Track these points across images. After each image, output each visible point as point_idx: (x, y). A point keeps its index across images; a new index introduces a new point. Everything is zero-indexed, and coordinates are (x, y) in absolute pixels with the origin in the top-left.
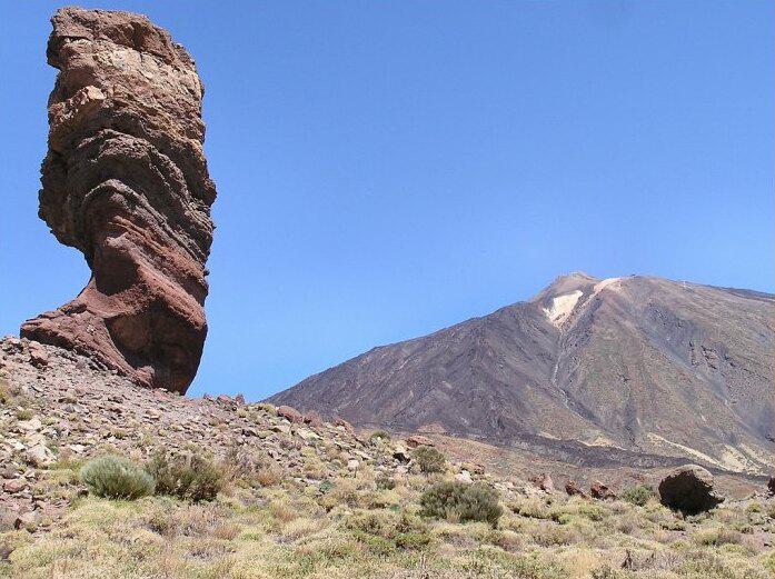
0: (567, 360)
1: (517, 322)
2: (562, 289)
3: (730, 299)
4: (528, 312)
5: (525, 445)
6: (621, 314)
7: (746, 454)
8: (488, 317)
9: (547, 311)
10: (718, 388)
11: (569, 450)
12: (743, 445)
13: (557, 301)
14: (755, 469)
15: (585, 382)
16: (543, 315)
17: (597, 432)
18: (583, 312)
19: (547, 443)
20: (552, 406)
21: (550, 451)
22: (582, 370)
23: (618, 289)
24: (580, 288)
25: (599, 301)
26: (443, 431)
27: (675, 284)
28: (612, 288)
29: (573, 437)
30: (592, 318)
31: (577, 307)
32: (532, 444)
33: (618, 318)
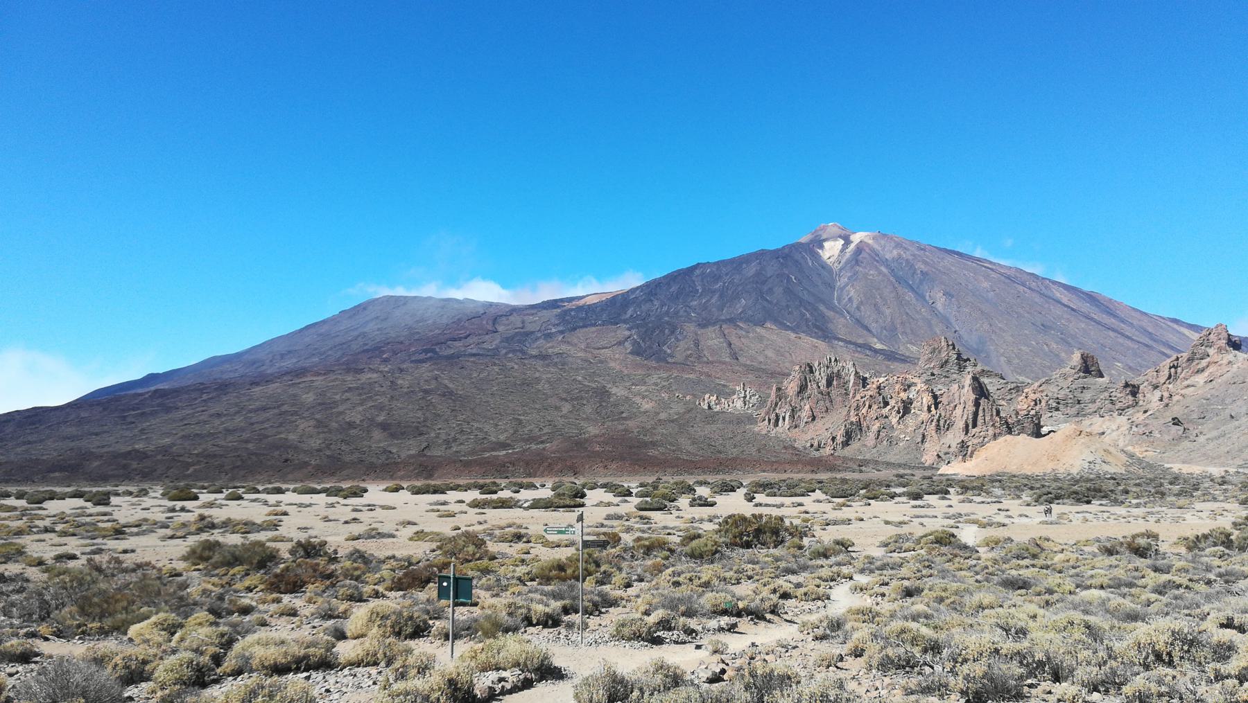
0: (842, 289)
1: (803, 257)
2: (824, 237)
3: (949, 259)
8: (778, 250)
10: (947, 320)
13: (826, 244)
15: (858, 308)
16: (818, 254)
18: (848, 255)
20: (842, 320)
22: (852, 294)
23: (870, 242)
24: (840, 237)
27: (912, 243)
31: (842, 251)
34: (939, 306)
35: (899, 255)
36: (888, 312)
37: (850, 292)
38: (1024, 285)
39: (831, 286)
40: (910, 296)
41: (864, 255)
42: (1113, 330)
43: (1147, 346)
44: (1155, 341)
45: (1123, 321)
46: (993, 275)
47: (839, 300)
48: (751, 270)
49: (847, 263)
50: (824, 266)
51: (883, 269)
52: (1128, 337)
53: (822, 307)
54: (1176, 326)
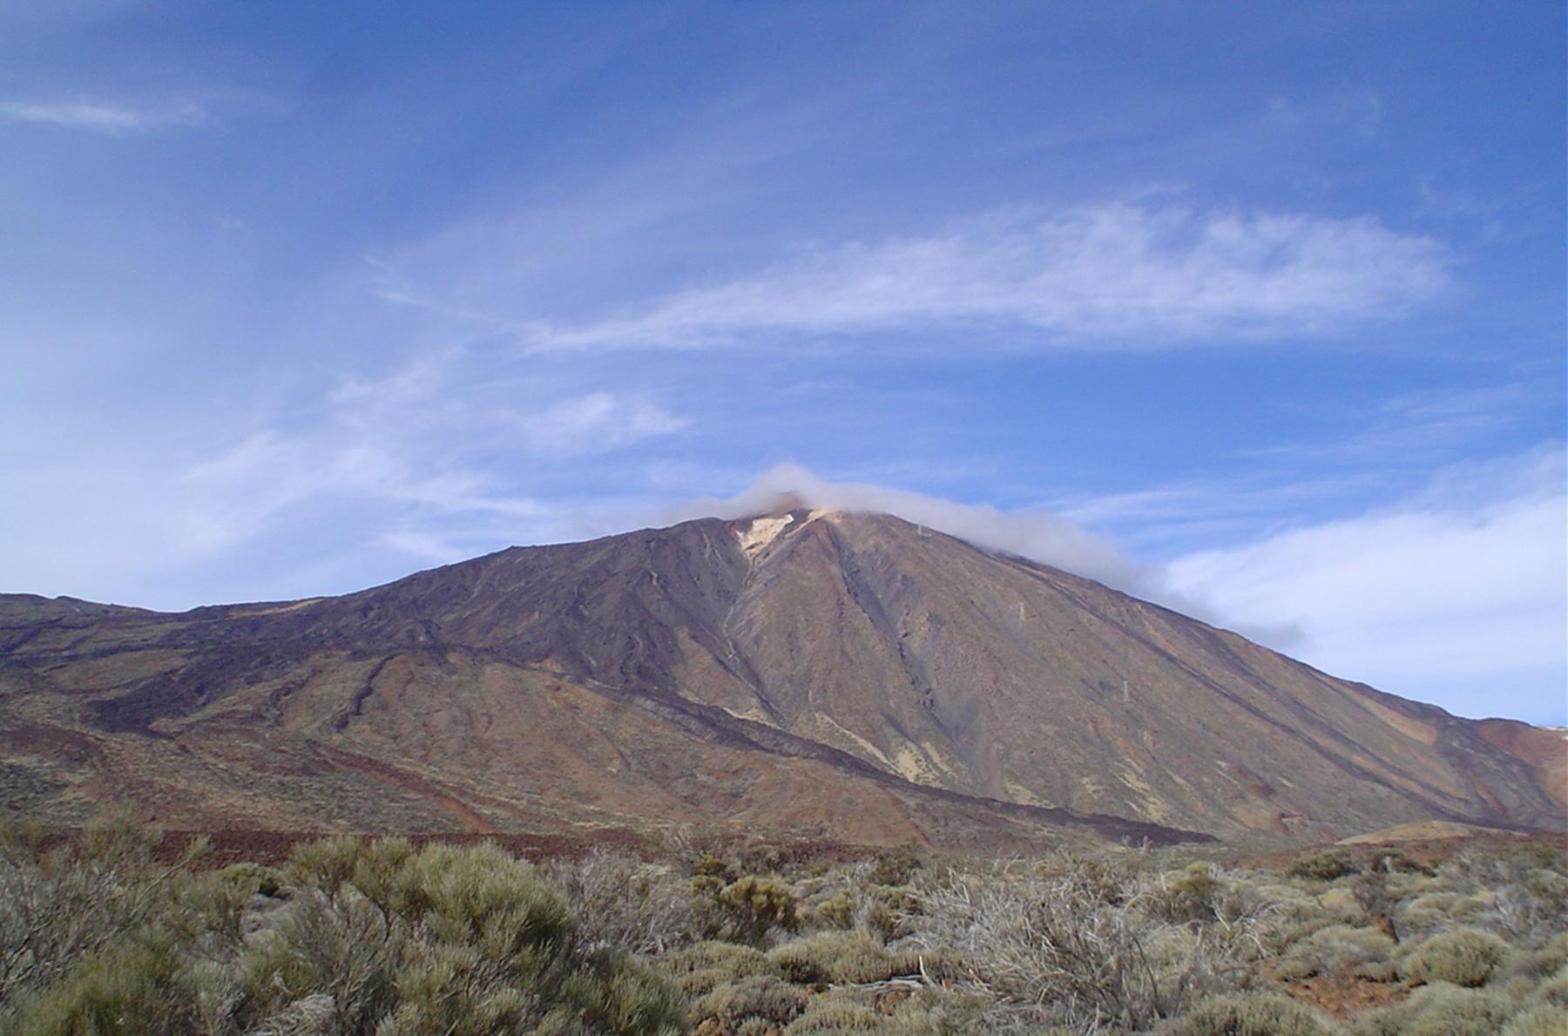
4: (723, 531)
5: (649, 704)
6: (830, 555)
7: (928, 757)
9: (740, 534)
11: (700, 717)
12: (927, 745)
14: (931, 779)
15: (757, 641)
17: (754, 701)
18: (785, 543)
19: (682, 707)
20: (708, 659)
21: (679, 717)
23: (837, 521)
25: (806, 535)
26: (559, 670)
28: (829, 519)
29: (720, 703)
30: (792, 554)
31: (780, 537)
32: (661, 704)
33: (824, 557)
34: (915, 644)
35: (877, 546)
36: (809, 647)
37: (757, 611)
38: (1093, 611)
39: (729, 597)
40: (861, 620)
41: (811, 542)
42: (1235, 699)
43: (1285, 728)
44: (1310, 722)
45: (1259, 683)
46: (1044, 590)
47: (732, 623)
48: (588, 563)
49: (777, 556)
50: (736, 562)
51: (835, 569)
52: (1258, 714)
53: (682, 635)
54: (1357, 697)
